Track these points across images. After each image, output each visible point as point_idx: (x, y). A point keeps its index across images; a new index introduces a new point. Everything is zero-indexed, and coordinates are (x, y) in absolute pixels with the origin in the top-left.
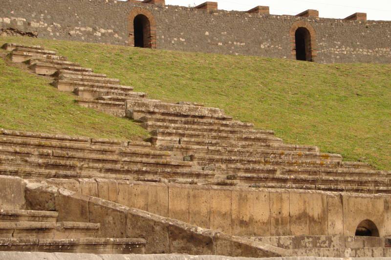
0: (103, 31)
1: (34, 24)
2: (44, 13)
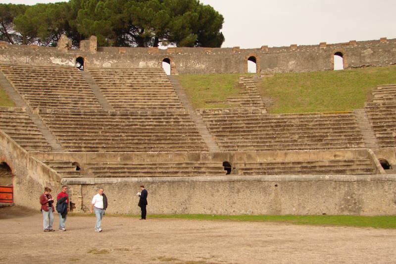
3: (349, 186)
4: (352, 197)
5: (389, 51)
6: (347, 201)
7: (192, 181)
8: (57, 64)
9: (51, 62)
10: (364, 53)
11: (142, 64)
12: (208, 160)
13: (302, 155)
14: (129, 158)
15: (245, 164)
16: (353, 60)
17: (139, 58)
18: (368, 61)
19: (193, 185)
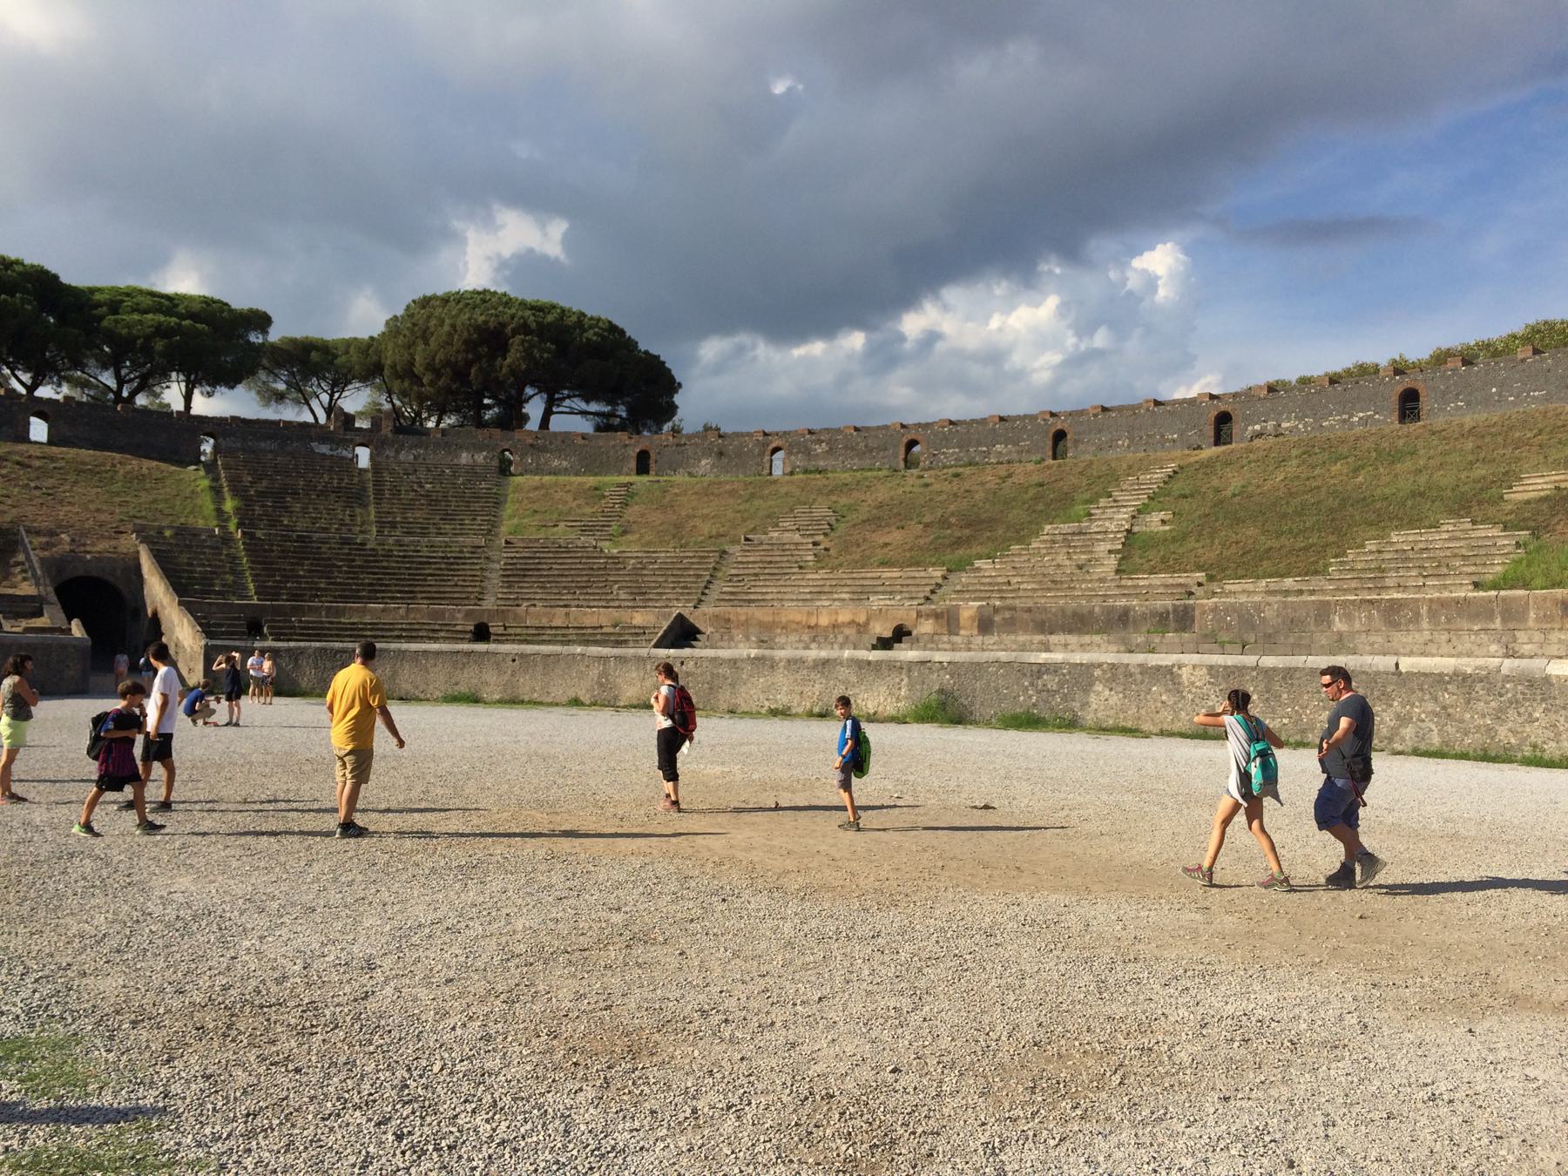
0: (1361, 415)
1: (1284, 425)
2: (1295, 412)
3: (604, 664)
4: (607, 680)
5: (853, 449)
6: (601, 685)
7: (399, 650)
8: (324, 454)
9: (312, 450)
10: (815, 450)
11: (464, 458)
12: (458, 619)
13: (588, 616)
14: (340, 612)
15: (505, 628)
16: (799, 461)
17: (461, 447)
18: (821, 463)
19: (401, 654)
